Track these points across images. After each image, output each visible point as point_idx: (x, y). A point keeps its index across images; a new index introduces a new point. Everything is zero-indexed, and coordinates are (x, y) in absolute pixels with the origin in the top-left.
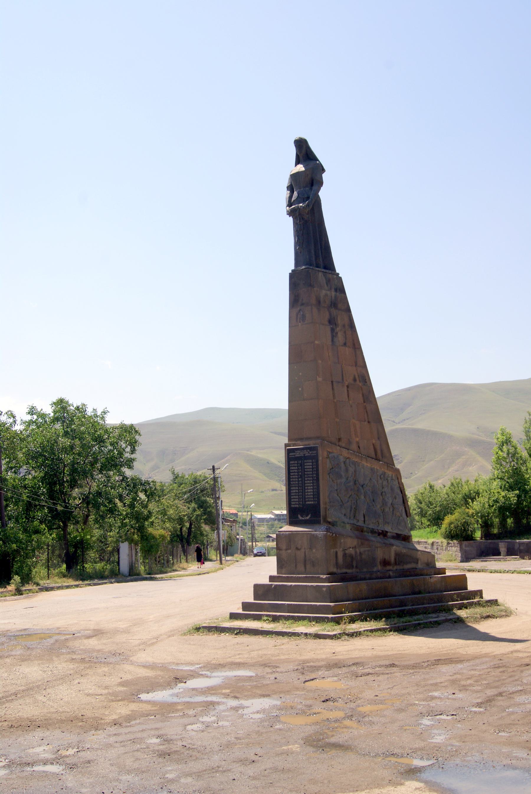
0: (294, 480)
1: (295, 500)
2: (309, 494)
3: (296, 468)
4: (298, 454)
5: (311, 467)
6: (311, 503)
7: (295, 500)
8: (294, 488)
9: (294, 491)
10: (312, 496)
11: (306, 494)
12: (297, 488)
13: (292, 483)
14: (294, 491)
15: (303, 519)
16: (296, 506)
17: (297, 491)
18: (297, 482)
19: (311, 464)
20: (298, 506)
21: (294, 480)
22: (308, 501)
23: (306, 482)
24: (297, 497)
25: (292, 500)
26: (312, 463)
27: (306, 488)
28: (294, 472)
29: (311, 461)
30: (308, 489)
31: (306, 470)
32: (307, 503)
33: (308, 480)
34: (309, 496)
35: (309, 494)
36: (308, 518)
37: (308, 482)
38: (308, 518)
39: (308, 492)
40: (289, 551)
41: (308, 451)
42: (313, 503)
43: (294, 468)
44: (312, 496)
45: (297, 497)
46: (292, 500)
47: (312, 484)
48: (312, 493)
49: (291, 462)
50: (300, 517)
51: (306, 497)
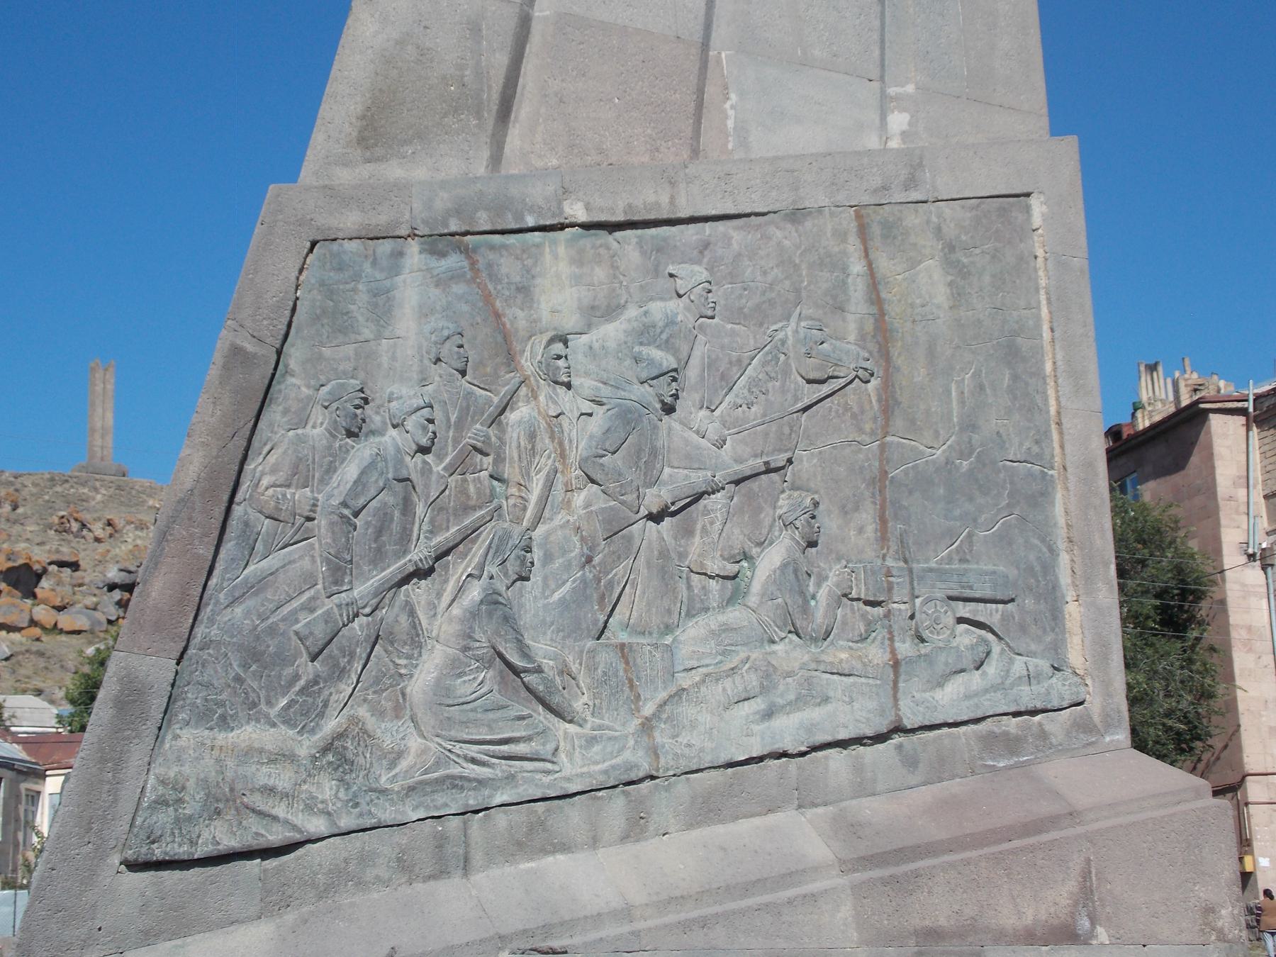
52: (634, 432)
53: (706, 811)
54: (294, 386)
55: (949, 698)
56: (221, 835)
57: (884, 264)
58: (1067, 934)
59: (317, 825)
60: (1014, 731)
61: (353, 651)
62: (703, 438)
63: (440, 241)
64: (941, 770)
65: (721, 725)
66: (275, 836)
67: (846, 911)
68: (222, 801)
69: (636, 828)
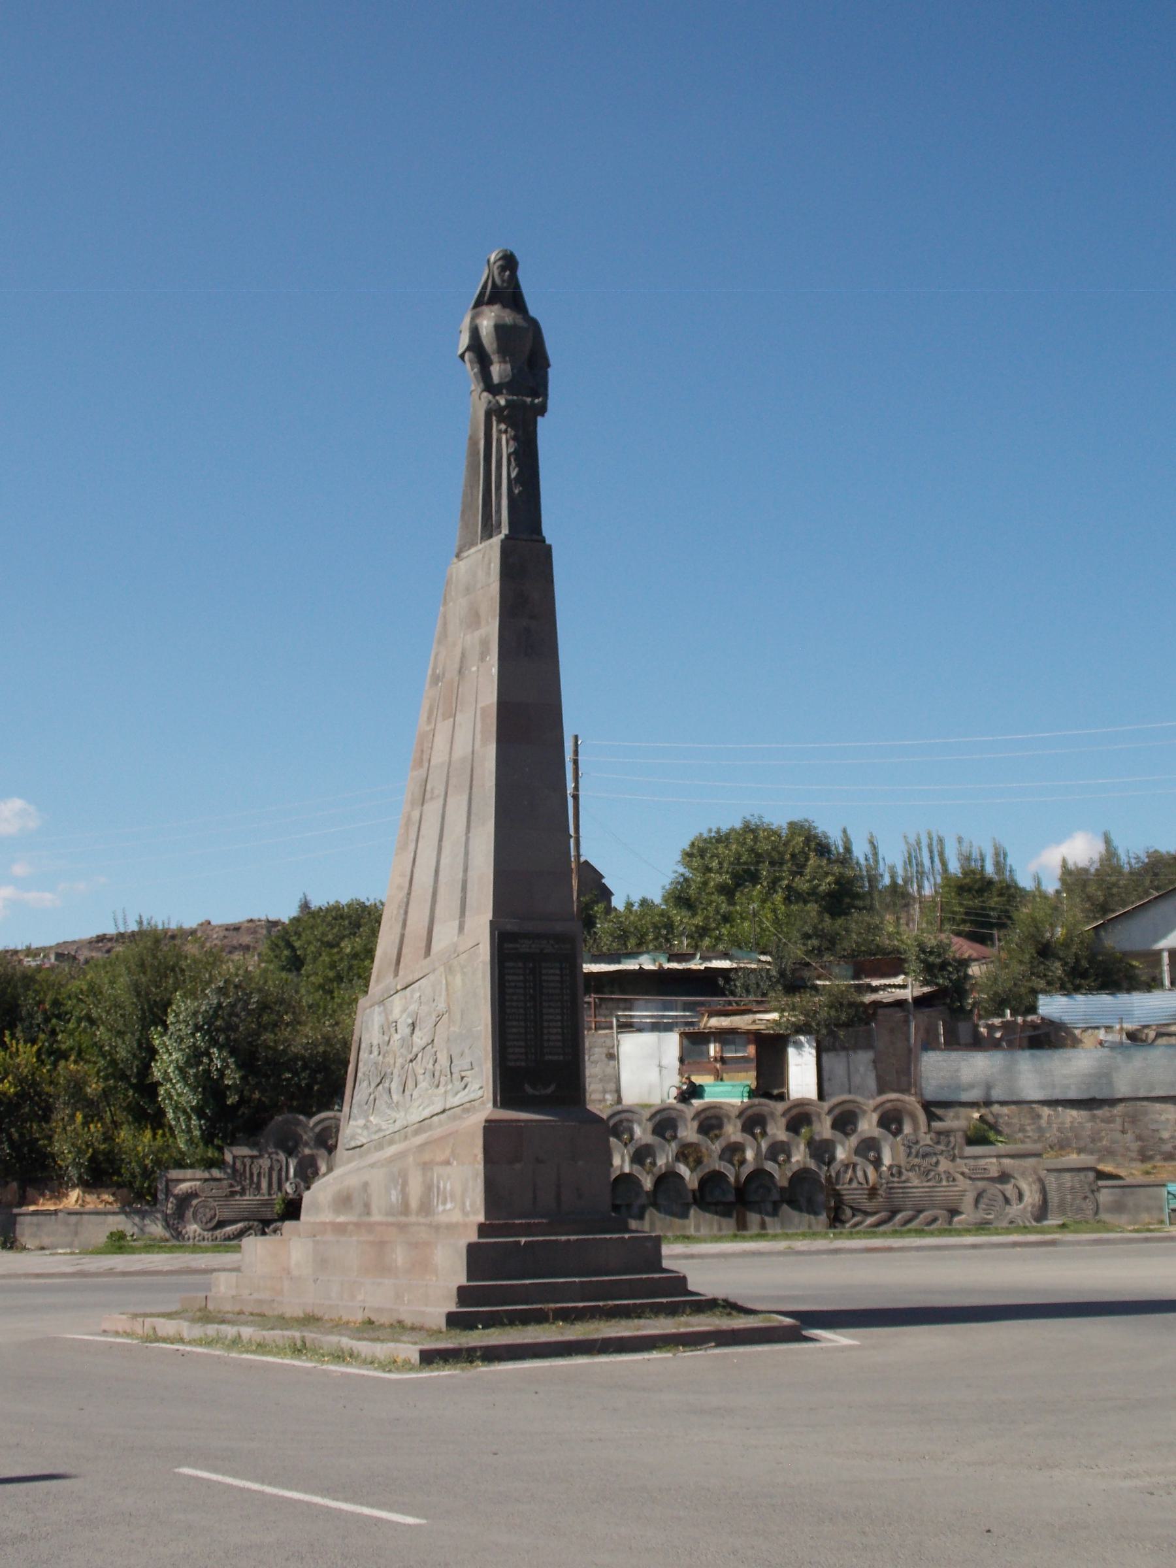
0: (514, 1004)
1: (517, 1050)
2: (553, 1037)
3: (521, 978)
4: (525, 947)
5: (558, 978)
6: (556, 1058)
7: (517, 1050)
8: (515, 1023)
9: (514, 1030)
10: (560, 1044)
11: (546, 1037)
12: (522, 1024)
13: (508, 1011)
14: (514, 1030)
15: (537, 1093)
16: (518, 1064)
17: (522, 1031)
18: (522, 1011)
19: (558, 972)
20: (523, 1064)
21: (514, 1004)
22: (551, 1054)
23: (545, 1011)
24: (522, 1044)
25: (510, 1050)
26: (561, 969)
27: (545, 1024)
28: (516, 987)
29: (558, 965)
30: (549, 1027)
31: (544, 984)
32: (548, 1057)
33: (550, 1007)
34: (551, 1044)
35: (553, 1037)
36: (549, 1091)
37: (551, 1011)
38: (549, 1091)
39: (549, 1033)
40: (518, 1166)
41: (552, 942)
42: (561, 1058)
43: (515, 978)
44: (560, 1044)
45: (522, 1044)
46: (510, 1050)
47: (559, 1017)
48: (559, 1037)
49: (508, 964)
50: (529, 1090)
51: (546, 1044)
52: (407, 1043)
53: (416, 1133)
54: (363, 1046)
55: (456, 1101)
56: (353, 1144)
57: (450, 978)
58: (448, 1163)
59: (364, 1141)
60: (467, 1108)
61: (372, 1103)
62: (419, 1039)
63: (381, 1002)
64: (455, 1118)
65: (415, 1115)
66: (359, 1144)
67: (411, 1159)
68: (353, 1138)
69: (406, 1138)
